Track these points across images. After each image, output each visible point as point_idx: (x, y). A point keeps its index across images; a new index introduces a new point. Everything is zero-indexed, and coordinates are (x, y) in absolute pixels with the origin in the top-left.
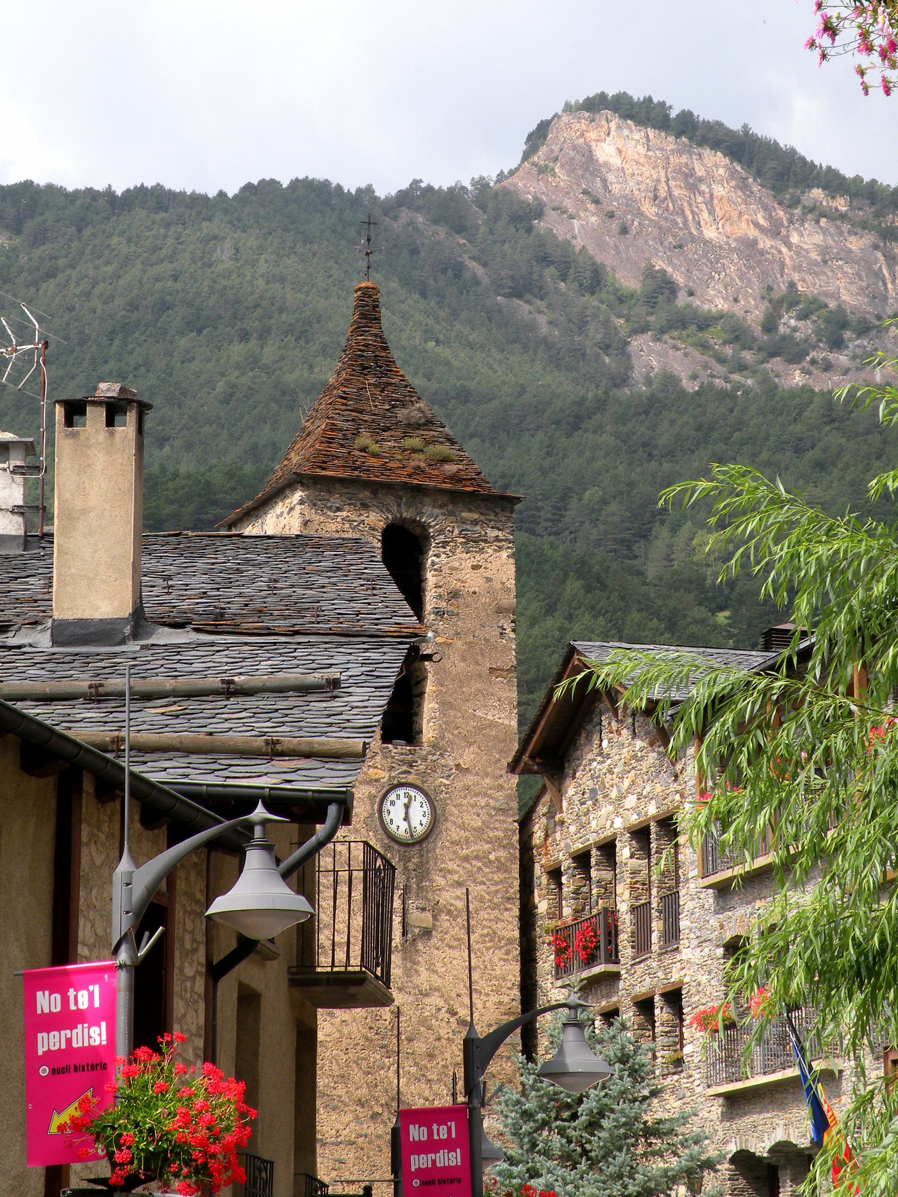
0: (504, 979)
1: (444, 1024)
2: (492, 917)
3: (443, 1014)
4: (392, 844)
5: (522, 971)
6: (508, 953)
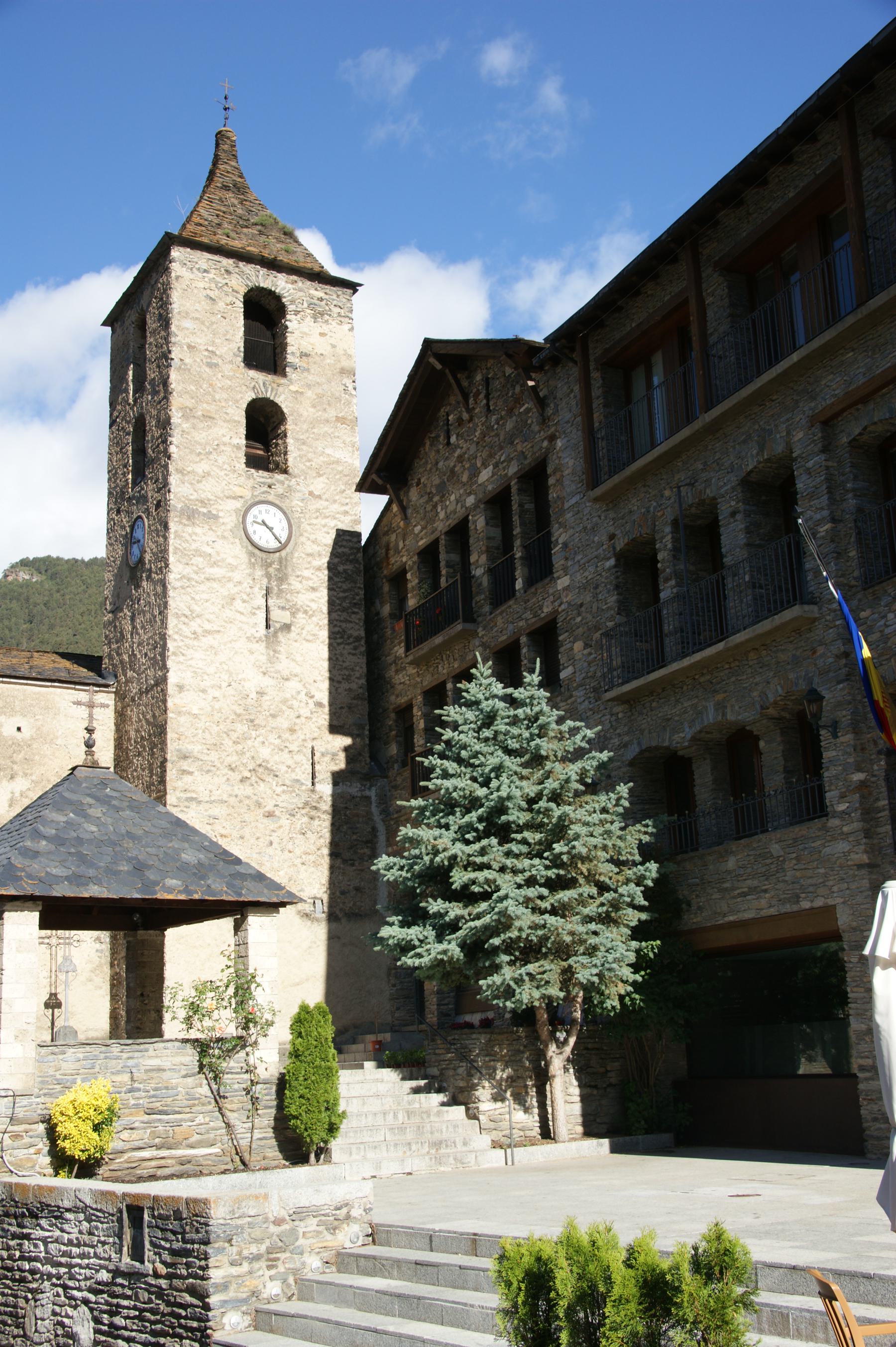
0: (353, 670)
1: (302, 704)
2: (342, 619)
3: (302, 696)
4: (257, 552)
5: (369, 664)
6: (355, 648)
